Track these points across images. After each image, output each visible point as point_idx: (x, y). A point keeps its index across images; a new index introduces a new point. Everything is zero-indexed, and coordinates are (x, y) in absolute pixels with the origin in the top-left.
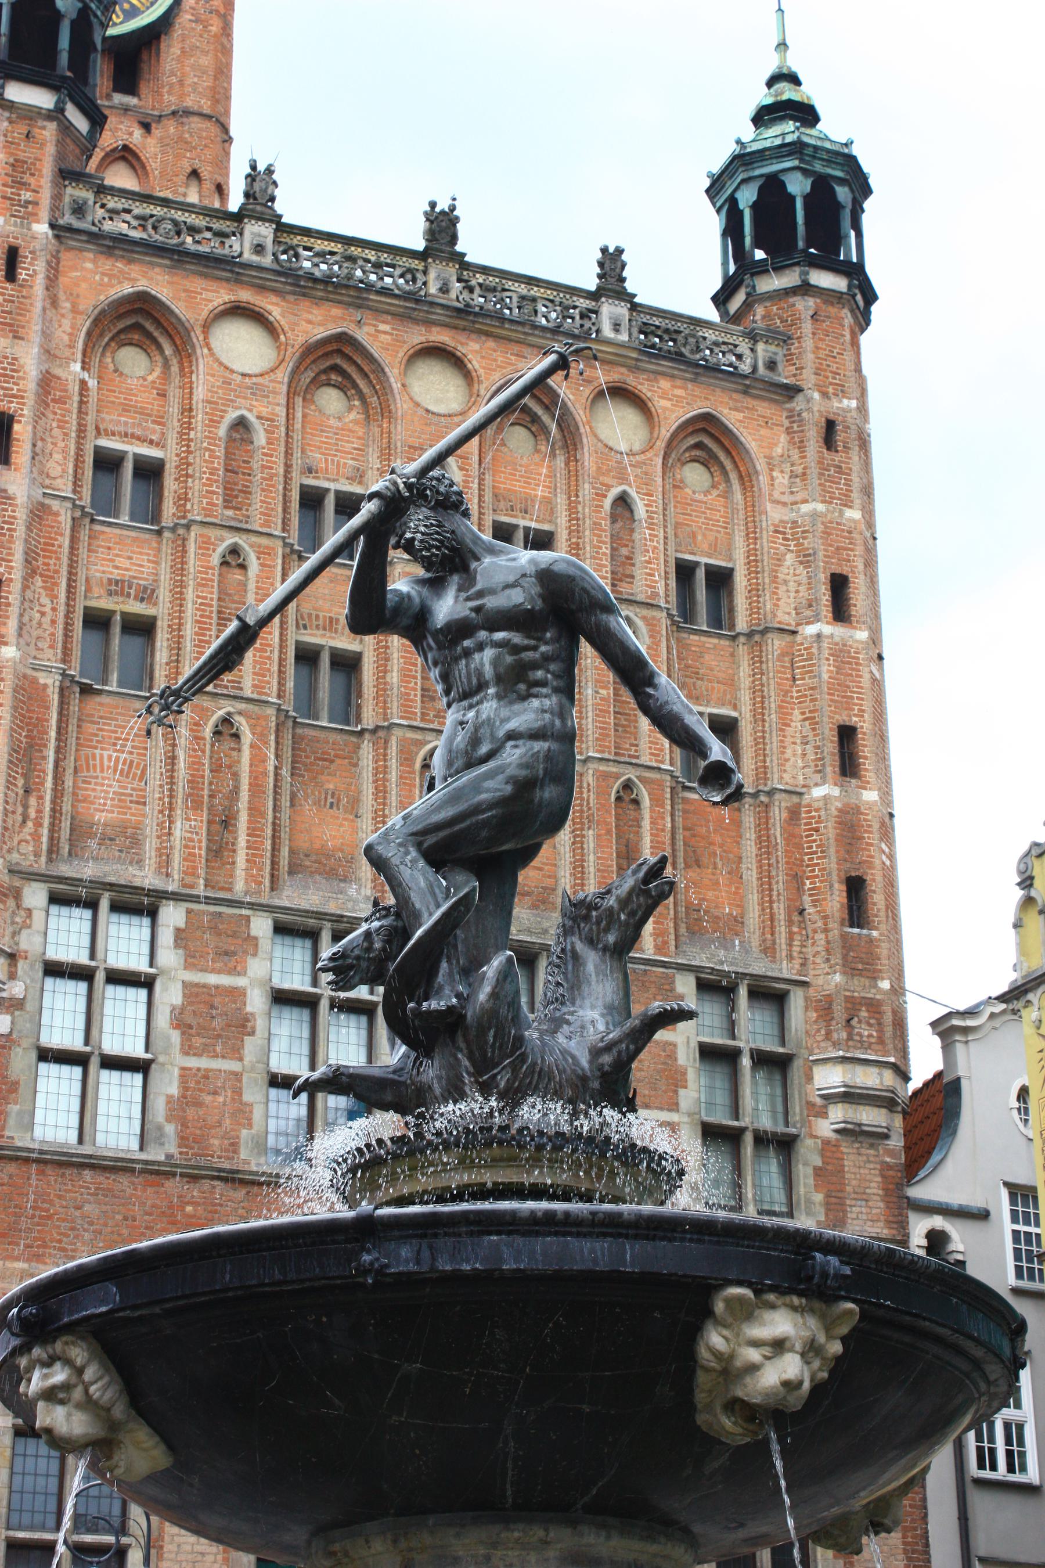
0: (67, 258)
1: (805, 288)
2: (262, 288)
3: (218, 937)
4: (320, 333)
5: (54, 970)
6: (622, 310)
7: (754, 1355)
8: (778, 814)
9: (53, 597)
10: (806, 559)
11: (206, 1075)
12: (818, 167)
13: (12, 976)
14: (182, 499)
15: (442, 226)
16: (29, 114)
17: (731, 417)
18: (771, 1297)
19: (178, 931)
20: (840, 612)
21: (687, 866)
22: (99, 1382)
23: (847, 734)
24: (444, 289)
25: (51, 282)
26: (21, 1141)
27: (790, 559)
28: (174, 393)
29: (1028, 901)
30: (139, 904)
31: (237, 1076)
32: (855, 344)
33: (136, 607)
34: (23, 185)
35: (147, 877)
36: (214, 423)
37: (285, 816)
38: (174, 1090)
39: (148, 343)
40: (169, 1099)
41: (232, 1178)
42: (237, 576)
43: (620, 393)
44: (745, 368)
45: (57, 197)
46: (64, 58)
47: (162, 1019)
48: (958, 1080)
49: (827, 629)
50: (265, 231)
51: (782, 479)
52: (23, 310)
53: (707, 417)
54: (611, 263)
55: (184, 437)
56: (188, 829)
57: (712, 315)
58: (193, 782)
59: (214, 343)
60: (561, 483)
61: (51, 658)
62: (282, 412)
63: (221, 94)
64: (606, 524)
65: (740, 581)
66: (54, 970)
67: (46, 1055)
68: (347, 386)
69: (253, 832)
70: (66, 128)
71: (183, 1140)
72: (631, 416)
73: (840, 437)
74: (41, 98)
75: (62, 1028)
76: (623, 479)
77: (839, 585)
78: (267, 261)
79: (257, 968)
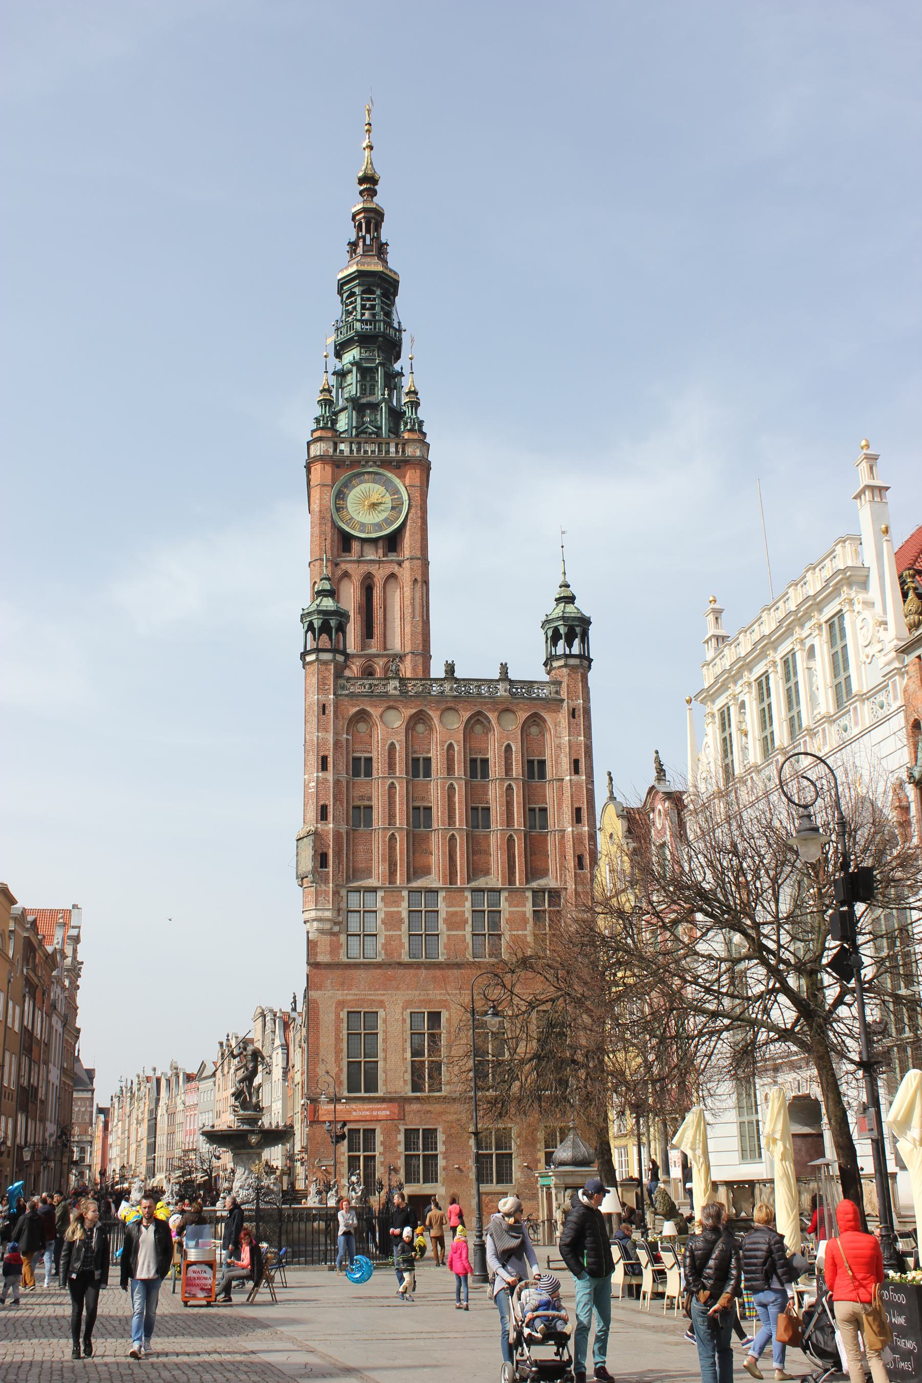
2: (396, 701)
4: (414, 711)
11: (392, 936)
12: (570, 623)
13: (339, 915)
16: (325, 663)
20: (577, 771)
21: (531, 855)
23: (578, 810)
25: (335, 712)
26: (345, 960)
27: (562, 755)
33: (367, 803)
34: (326, 684)
35: (372, 882)
38: (383, 941)
39: (365, 721)
41: (400, 964)
43: (507, 710)
52: (328, 723)
54: (504, 668)
57: (539, 674)
58: (383, 855)
59: (384, 719)
62: (404, 738)
64: (503, 755)
65: (548, 764)
71: (386, 954)
72: (511, 716)
76: (508, 739)
77: (576, 762)
78: (397, 693)
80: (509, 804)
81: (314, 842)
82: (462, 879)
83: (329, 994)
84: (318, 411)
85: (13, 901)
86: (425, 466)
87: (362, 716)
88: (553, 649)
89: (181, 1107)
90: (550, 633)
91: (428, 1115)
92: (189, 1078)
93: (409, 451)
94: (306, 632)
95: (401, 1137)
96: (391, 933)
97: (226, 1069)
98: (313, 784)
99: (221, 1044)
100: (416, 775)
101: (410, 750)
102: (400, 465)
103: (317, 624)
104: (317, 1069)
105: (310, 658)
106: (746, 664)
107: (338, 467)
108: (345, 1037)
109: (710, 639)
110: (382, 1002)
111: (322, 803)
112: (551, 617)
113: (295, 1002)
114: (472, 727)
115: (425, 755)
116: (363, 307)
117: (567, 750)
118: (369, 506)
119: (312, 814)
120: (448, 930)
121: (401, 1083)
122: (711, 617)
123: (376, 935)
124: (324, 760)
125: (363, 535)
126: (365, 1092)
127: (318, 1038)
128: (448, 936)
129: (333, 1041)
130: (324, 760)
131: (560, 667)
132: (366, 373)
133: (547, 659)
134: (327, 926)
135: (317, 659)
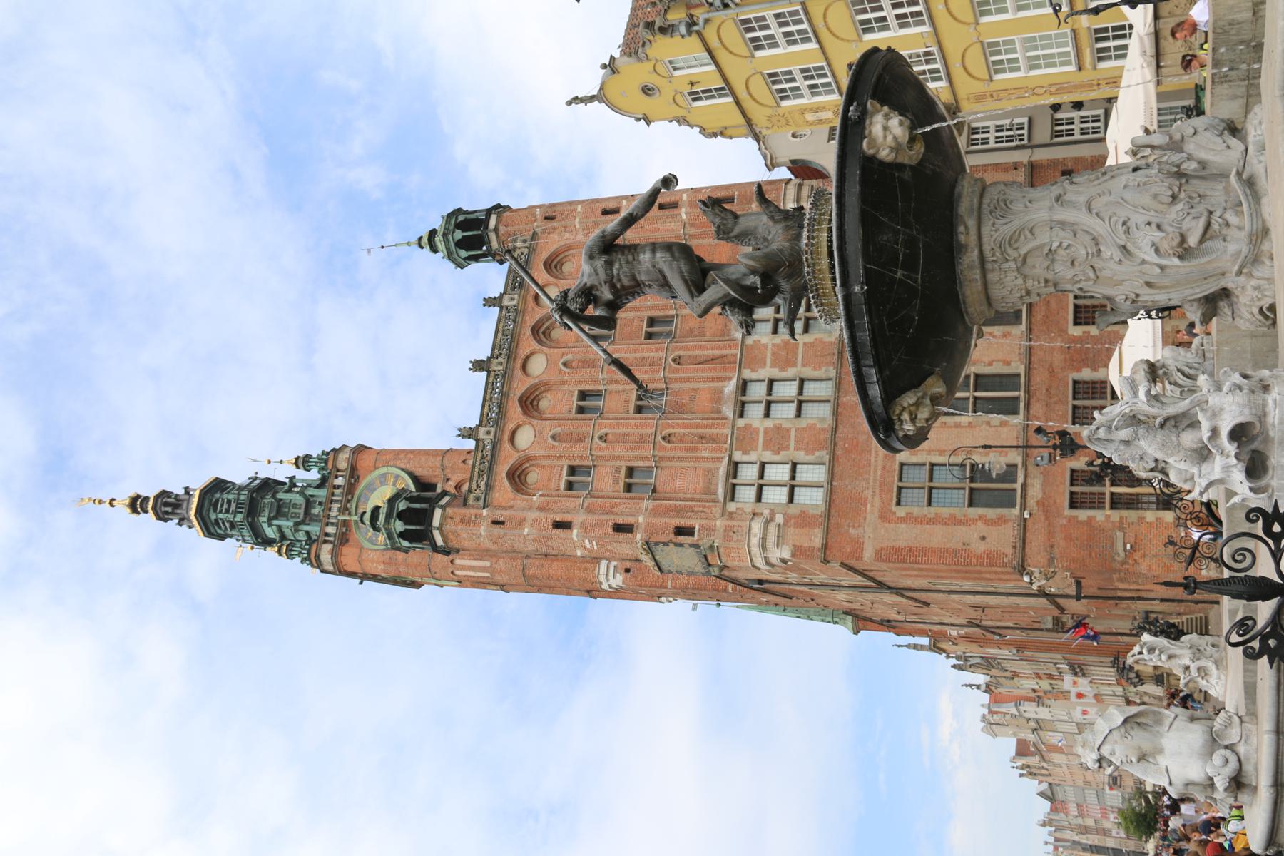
0: (495, 503)
1: (496, 230)
3: (745, 439)
4: (519, 409)
5: (759, 498)
6: (506, 297)
7: (890, 138)
8: (693, 231)
11: (797, 441)
14: (582, 458)
15: (478, 365)
16: (443, 517)
17: (544, 255)
18: (867, 132)
22: (909, 399)
24: (501, 364)
29: (722, 134)
30: (734, 467)
31: (797, 430)
32: (516, 211)
36: (553, 447)
37: (699, 416)
40: (807, 454)
41: (835, 430)
42: (610, 437)
44: (526, 251)
45: (473, 507)
46: (423, 506)
47: (777, 458)
48: (793, 162)
50: (482, 430)
51: (567, 235)
53: (545, 264)
54: (489, 302)
55: (559, 458)
56: (705, 451)
58: (688, 450)
61: (643, 504)
63: (435, 453)
66: (759, 498)
67: (791, 500)
70: (448, 504)
71: (820, 449)
73: (550, 214)
74: (438, 513)
75: (782, 495)
78: (493, 430)
79: (756, 424)
81: (657, 544)
82: (730, 347)
84: (298, 560)
86: (361, 449)
90: (463, 253)
91: (1053, 391)
93: (343, 464)
97: (1044, 772)
99: (1021, 775)
100: (595, 409)
101: (566, 416)
102: (353, 472)
103: (399, 526)
104: (978, 552)
107: (347, 541)
108: (932, 510)
111: (610, 530)
113: (970, 686)
114: (551, 341)
115: (575, 398)
116: (227, 511)
120: (794, 365)
121: (1005, 429)
124: (558, 525)
126: (1015, 481)
127: (932, 550)
128: (803, 365)
129: (939, 530)
130: (558, 525)
131: (497, 236)
132: (280, 510)
134: (772, 529)
135: (439, 528)
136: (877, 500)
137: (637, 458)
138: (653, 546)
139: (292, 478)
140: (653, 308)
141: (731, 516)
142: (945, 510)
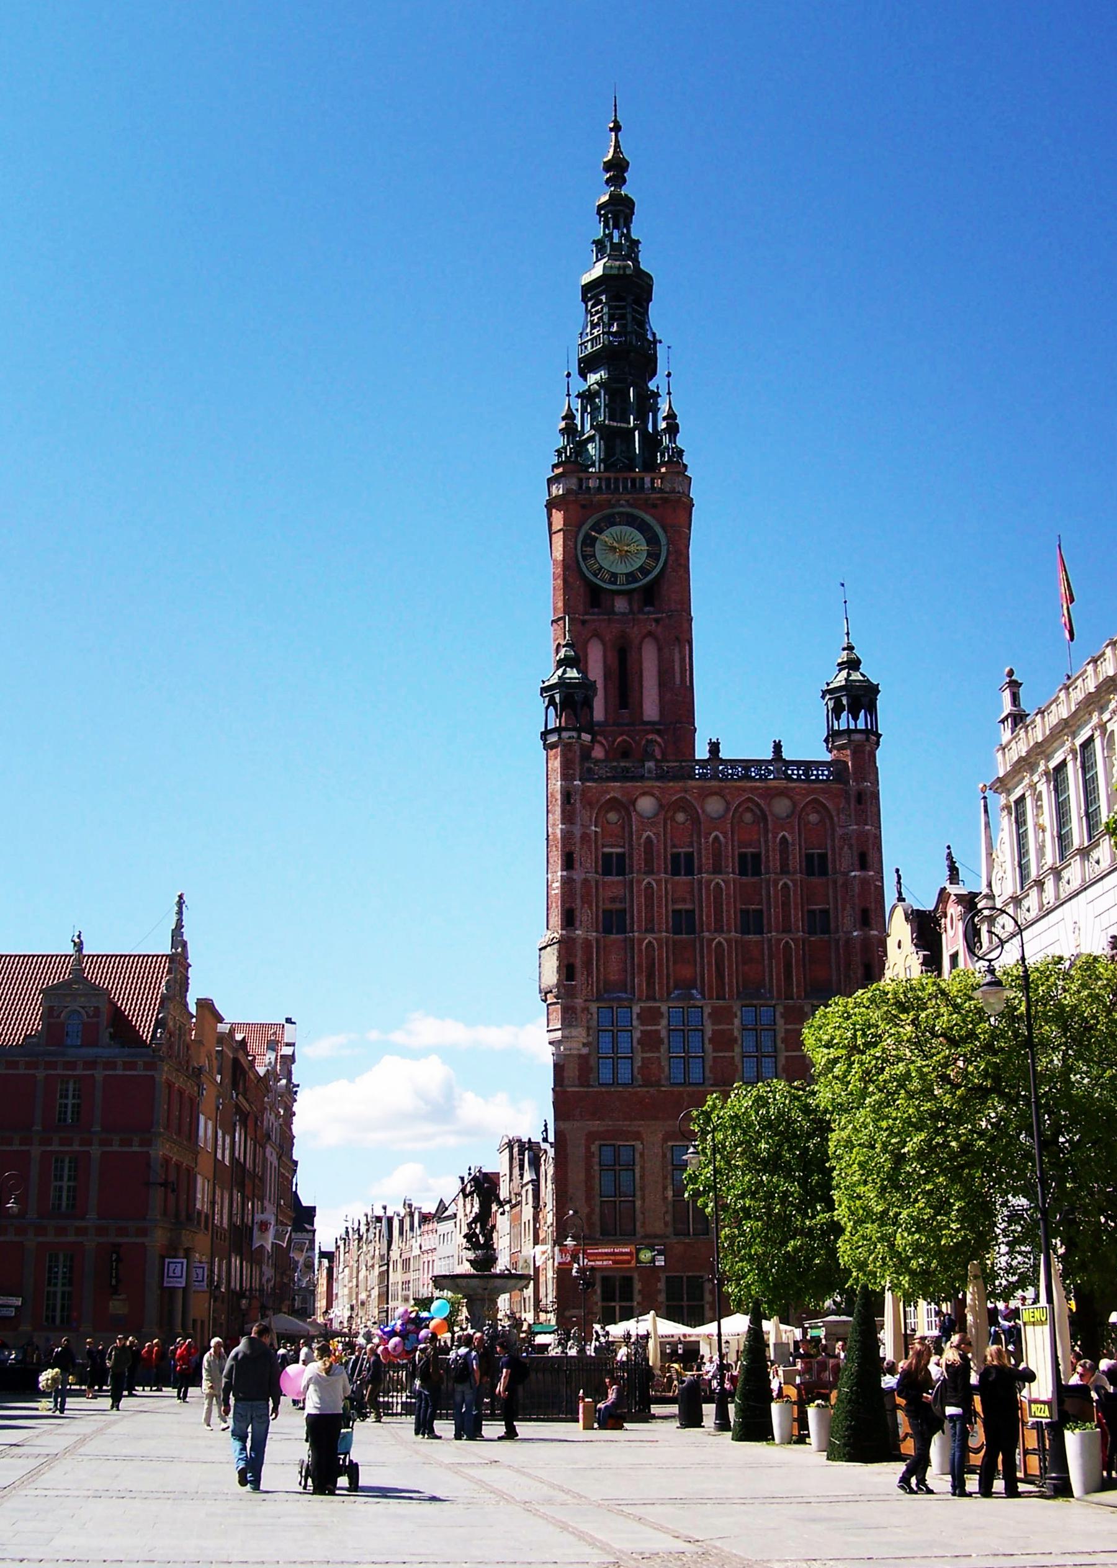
9: (591, 910)
10: (851, 847)
11: (649, 1058)
15: (714, 747)
19: (638, 1014)
20: (863, 865)
28: (626, 829)
31: (658, 1058)
39: (618, 811)
49: (857, 873)
54: (778, 747)
58: (640, 966)
60: (762, 831)
64: (778, 848)
68: (685, 811)
69: (660, 978)
79: (664, 1022)
80: (786, 904)
83: (577, 1124)
85: (220, 1020)
87: (614, 804)
88: (836, 723)
89: (416, 1252)
90: (831, 704)
92: (425, 1218)
94: (547, 708)
95: (661, 1285)
96: (648, 1055)
98: (558, 884)
99: (462, 1179)
105: (553, 738)
106: (1041, 750)
109: (1006, 718)
110: (639, 1133)
112: (832, 686)
113: (546, 1130)
117: (853, 841)
118: (622, 552)
119: (556, 919)
120: (715, 1051)
121: (662, 1225)
122: (1007, 695)
123: (631, 1058)
125: (614, 587)
129: (582, 1176)
133: (828, 735)
136: (601, 1129)
137: (632, 918)
138: (556, 946)
139: (658, 395)
140: (769, 915)
141: (586, 1009)
142: (597, 1182)
